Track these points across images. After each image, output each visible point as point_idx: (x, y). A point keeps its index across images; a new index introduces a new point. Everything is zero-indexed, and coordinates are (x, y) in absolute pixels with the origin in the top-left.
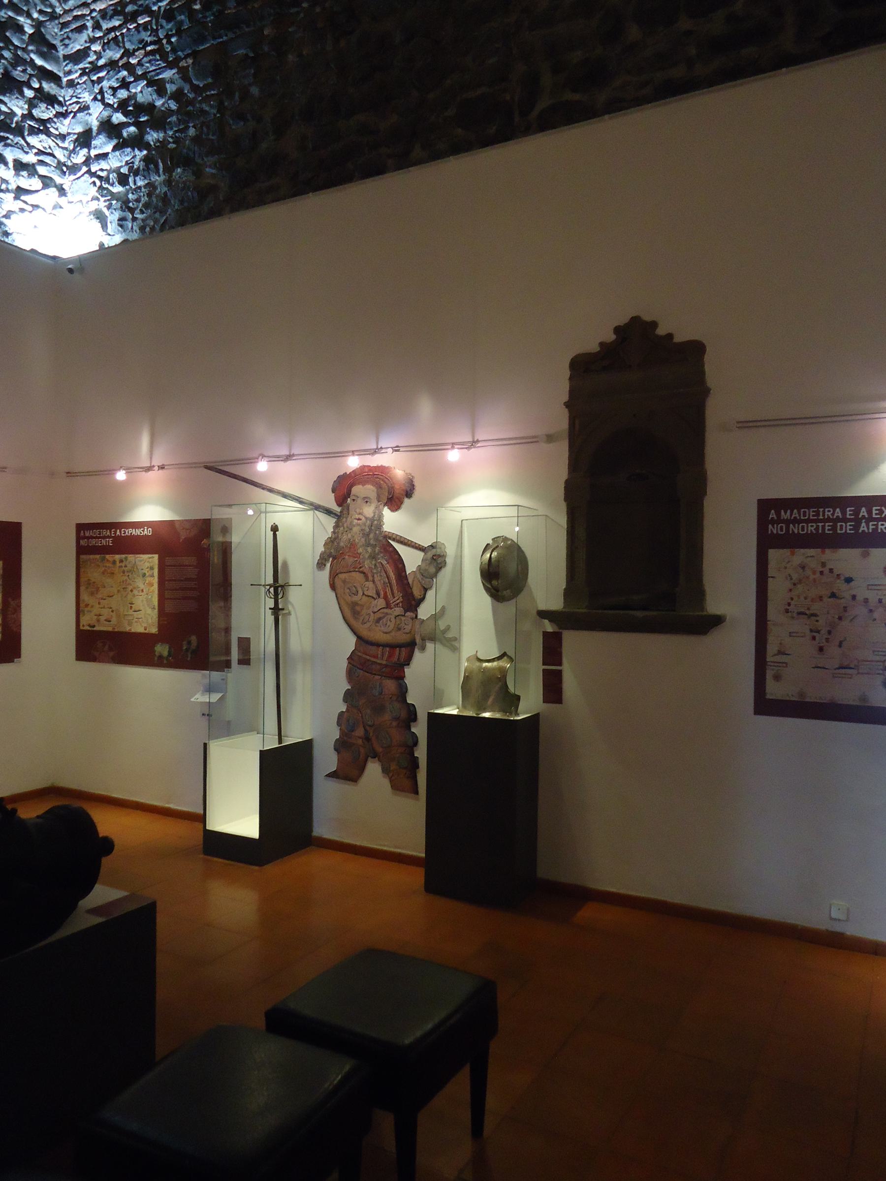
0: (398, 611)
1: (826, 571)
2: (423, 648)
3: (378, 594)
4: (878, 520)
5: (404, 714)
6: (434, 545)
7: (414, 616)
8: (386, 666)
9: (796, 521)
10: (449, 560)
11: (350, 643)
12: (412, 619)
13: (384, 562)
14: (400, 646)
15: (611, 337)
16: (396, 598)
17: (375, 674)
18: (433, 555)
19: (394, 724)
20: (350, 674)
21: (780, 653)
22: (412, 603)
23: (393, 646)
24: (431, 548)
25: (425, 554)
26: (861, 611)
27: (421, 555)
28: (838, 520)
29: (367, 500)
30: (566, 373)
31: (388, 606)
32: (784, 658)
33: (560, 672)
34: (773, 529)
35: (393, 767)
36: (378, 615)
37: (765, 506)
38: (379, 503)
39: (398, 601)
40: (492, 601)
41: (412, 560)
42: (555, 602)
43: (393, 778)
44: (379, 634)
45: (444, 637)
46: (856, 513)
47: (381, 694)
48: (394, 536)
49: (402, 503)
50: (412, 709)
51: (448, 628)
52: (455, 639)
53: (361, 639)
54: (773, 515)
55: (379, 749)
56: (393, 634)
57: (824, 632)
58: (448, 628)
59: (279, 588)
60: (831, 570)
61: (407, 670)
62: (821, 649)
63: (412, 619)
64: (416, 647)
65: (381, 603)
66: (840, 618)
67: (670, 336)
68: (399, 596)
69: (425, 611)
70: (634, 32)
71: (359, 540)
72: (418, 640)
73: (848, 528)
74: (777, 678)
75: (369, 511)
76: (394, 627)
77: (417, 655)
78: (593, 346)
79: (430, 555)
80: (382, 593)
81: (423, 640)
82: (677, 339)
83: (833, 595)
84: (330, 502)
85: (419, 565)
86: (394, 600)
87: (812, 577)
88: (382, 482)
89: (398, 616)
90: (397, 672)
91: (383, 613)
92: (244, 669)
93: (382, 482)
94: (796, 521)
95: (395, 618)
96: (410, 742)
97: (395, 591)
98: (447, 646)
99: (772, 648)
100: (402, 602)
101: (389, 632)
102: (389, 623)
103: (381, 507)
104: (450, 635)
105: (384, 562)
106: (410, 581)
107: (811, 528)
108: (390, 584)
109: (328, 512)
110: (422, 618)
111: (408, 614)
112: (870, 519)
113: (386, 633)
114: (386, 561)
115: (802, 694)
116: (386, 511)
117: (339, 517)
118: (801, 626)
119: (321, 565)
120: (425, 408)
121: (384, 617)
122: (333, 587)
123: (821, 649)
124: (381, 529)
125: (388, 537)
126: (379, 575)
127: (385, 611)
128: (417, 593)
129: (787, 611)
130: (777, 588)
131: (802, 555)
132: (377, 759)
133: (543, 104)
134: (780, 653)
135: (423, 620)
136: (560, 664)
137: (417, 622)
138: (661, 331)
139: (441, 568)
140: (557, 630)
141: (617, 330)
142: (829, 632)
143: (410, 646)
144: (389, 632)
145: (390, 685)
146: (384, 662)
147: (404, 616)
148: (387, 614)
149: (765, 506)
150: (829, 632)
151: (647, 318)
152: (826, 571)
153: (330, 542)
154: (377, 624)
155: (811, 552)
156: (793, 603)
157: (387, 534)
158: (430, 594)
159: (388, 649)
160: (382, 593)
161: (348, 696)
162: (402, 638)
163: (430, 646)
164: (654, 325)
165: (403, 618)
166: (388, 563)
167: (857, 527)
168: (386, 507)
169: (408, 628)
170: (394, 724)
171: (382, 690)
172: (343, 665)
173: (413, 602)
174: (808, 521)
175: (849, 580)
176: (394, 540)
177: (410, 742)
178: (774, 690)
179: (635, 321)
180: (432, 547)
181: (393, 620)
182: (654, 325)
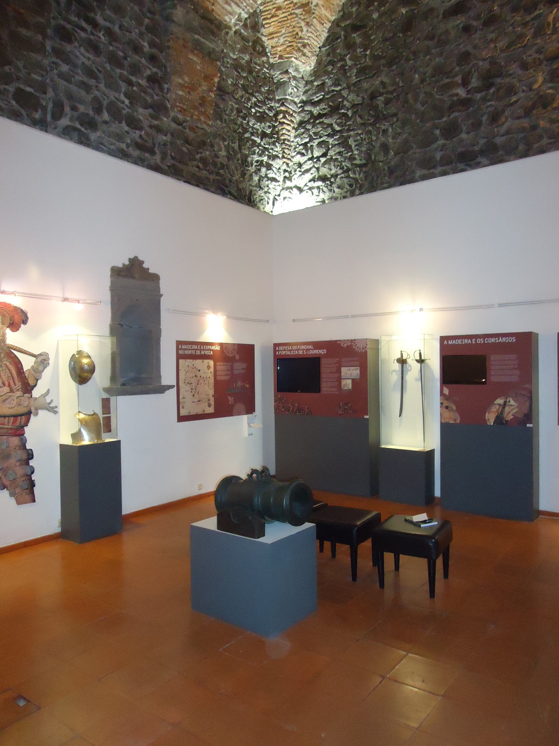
0: (19, 393)
1: (194, 368)
2: (36, 414)
3: (4, 384)
4: (206, 350)
5: (25, 457)
6: (42, 353)
7: (30, 396)
8: (11, 429)
9: (186, 349)
10: (51, 362)
12: (29, 398)
13: (8, 364)
14: (21, 415)
15: (127, 263)
16: (16, 386)
17: (3, 436)
18: (42, 360)
19: (18, 464)
21: (183, 398)
22: (28, 388)
23: (15, 416)
24: (40, 355)
25: (36, 359)
26: (202, 381)
27: (34, 359)
28: (196, 350)
30: (109, 273)
31: (12, 391)
32: (184, 400)
33: (110, 416)
34: (180, 352)
35: (18, 490)
36: (4, 397)
37: (179, 343)
38: (3, 326)
39: (19, 388)
40: (76, 385)
41: (27, 363)
42: (107, 383)
43: (18, 498)
45: (50, 407)
46: (200, 347)
47: (8, 447)
48: (15, 347)
49: (20, 327)
50: (30, 452)
51: (52, 401)
52: (56, 407)
54: (180, 347)
55: (7, 483)
56: (16, 408)
57: (194, 389)
58: (52, 401)
60: (195, 367)
61: (28, 430)
62: (193, 395)
63: (29, 398)
64: (32, 414)
65: (6, 389)
66: (198, 384)
67: (148, 269)
68: (19, 385)
69: (36, 393)
70: (106, 116)
72: (33, 410)
73: (198, 353)
74: (183, 407)
76: (16, 404)
78: (121, 266)
79: (40, 359)
80: (7, 383)
81: (36, 409)
82: (151, 271)
83: (196, 376)
85: (33, 366)
86: (15, 387)
87: (191, 370)
88: (5, 313)
89: (19, 397)
90: (19, 432)
91: (8, 395)
93: (5, 313)
94: (186, 349)
95: (17, 398)
96: (29, 473)
97: (17, 382)
98: (51, 412)
99: (181, 397)
100: (21, 388)
101: (13, 407)
102: (12, 402)
103: (5, 328)
104: (52, 405)
105: (8, 364)
106: (27, 375)
107: (190, 352)
108: (12, 376)
110: (36, 397)
111: (26, 395)
112: (203, 350)
113: (10, 408)
114: (10, 362)
115: (189, 412)
116: (8, 331)
118: (188, 388)
120: (34, 273)
121: (8, 398)
123: (193, 395)
124: (4, 342)
125: (10, 347)
126: (4, 371)
127: (10, 394)
128: (31, 382)
129: (185, 382)
130: (182, 373)
131: (189, 362)
132: (5, 489)
133: (64, 122)
134: (183, 398)
135: (36, 398)
136: (110, 413)
137: (32, 400)
138: (145, 266)
139: (46, 367)
140: (108, 397)
141: (130, 260)
142: (195, 389)
143: (28, 414)
144: (13, 407)
145: (15, 441)
146: (10, 427)
147: (23, 396)
148: (11, 396)
149: (179, 343)
150: (195, 389)
151: (141, 258)
152: (194, 368)
154: (4, 403)
155: (191, 360)
156: (186, 379)
157: (9, 346)
158: (39, 382)
159: (12, 418)
160: (7, 383)
162: (24, 410)
163: (41, 412)
164: (143, 262)
165: (22, 398)
166: (10, 364)
167: (201, 352)
168: (8, 329)
169: (26, 404)
170: (18, 464)
171: (9, 444)
173: (29, 388)
174: (189, 349)
175: (199, 371)
176: (14, 350)
177: (29, 473)
178: (183, 413)
179: (136, 258)
180: (40, 355)
181: (16, 400)
182: (143, 262)
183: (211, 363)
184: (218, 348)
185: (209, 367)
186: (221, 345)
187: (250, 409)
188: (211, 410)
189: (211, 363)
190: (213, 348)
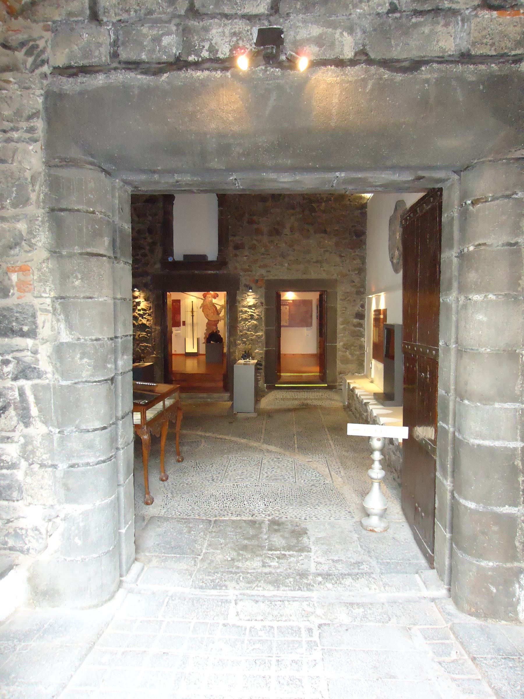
11: (207, 321)
20: (207, 326)
23: (215, 321)
29: (210, 297)
44: (212, 319)
53: (208, 320)
59: (192, 311)
71: (208, 304)
75: (210, 299)
77: (220, 322)
84: (202, 297)
92: (184, 326)
109: (202, 299)
116: (213, 299)
117: (204, 300)
119: (200, 308)
122: (203, 311)
128: (219, 312)
145: (215, 327)
153: (202, 304)
161: (206, 330)
162: (217, 320)
172: (206, 325)
183: (288, 307)
184: (291, 302)
185: (286, 308)
186: (293, 300)
187: (311, 325)
188: (287, 324)
189: (288, 307)
190: (289, 301)
